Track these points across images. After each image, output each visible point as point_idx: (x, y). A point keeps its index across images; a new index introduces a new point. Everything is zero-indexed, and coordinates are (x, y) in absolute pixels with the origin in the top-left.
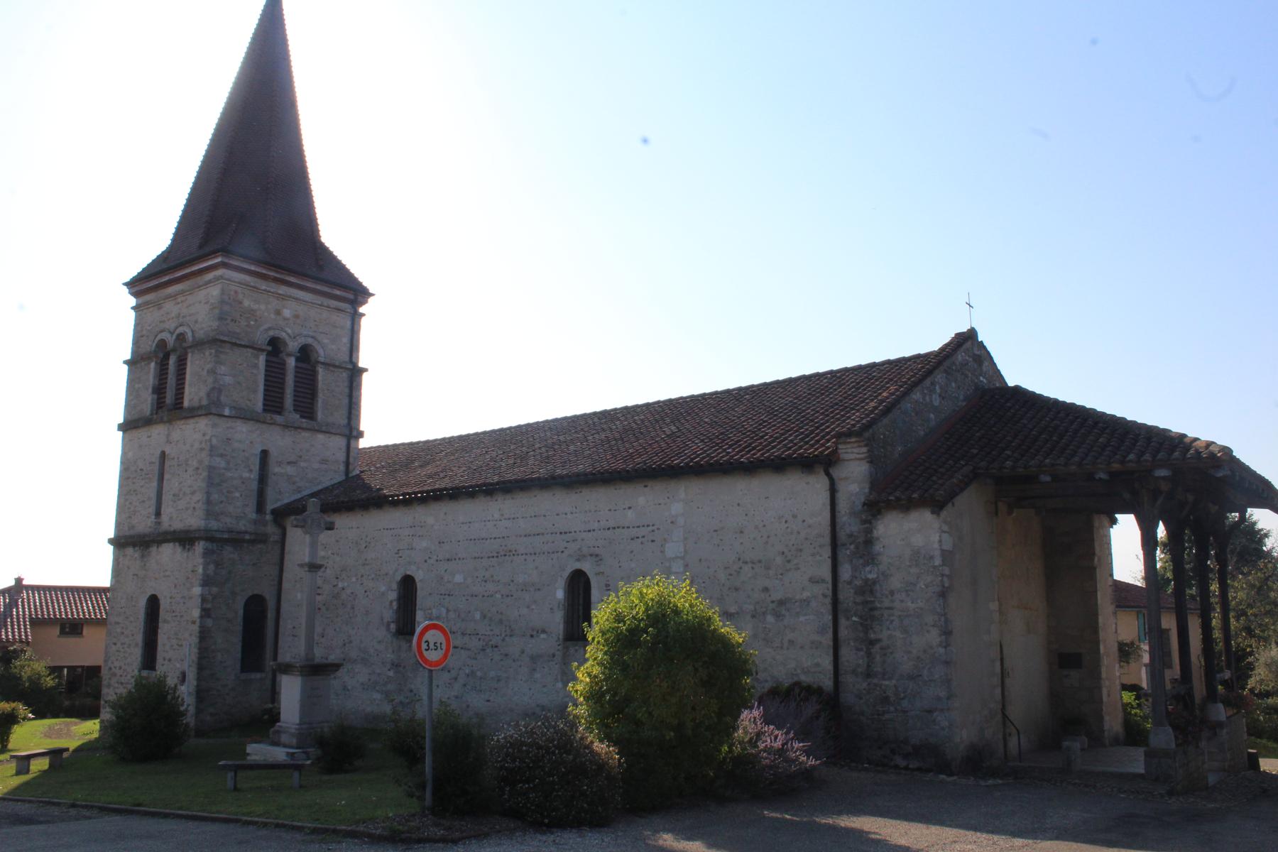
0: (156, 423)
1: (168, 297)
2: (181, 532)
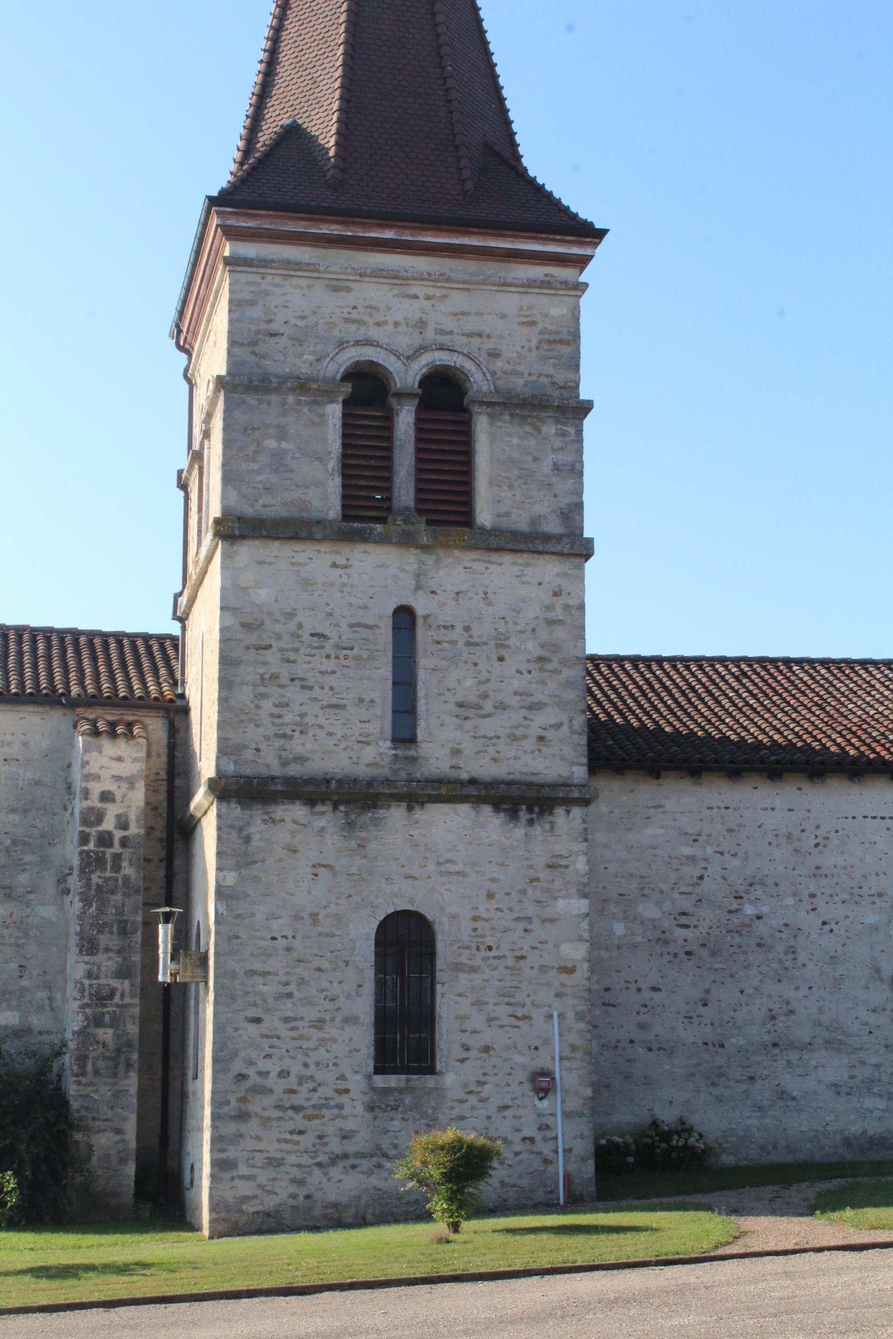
0: (383, 540)
1: (378, 274)
2: (494, 784)
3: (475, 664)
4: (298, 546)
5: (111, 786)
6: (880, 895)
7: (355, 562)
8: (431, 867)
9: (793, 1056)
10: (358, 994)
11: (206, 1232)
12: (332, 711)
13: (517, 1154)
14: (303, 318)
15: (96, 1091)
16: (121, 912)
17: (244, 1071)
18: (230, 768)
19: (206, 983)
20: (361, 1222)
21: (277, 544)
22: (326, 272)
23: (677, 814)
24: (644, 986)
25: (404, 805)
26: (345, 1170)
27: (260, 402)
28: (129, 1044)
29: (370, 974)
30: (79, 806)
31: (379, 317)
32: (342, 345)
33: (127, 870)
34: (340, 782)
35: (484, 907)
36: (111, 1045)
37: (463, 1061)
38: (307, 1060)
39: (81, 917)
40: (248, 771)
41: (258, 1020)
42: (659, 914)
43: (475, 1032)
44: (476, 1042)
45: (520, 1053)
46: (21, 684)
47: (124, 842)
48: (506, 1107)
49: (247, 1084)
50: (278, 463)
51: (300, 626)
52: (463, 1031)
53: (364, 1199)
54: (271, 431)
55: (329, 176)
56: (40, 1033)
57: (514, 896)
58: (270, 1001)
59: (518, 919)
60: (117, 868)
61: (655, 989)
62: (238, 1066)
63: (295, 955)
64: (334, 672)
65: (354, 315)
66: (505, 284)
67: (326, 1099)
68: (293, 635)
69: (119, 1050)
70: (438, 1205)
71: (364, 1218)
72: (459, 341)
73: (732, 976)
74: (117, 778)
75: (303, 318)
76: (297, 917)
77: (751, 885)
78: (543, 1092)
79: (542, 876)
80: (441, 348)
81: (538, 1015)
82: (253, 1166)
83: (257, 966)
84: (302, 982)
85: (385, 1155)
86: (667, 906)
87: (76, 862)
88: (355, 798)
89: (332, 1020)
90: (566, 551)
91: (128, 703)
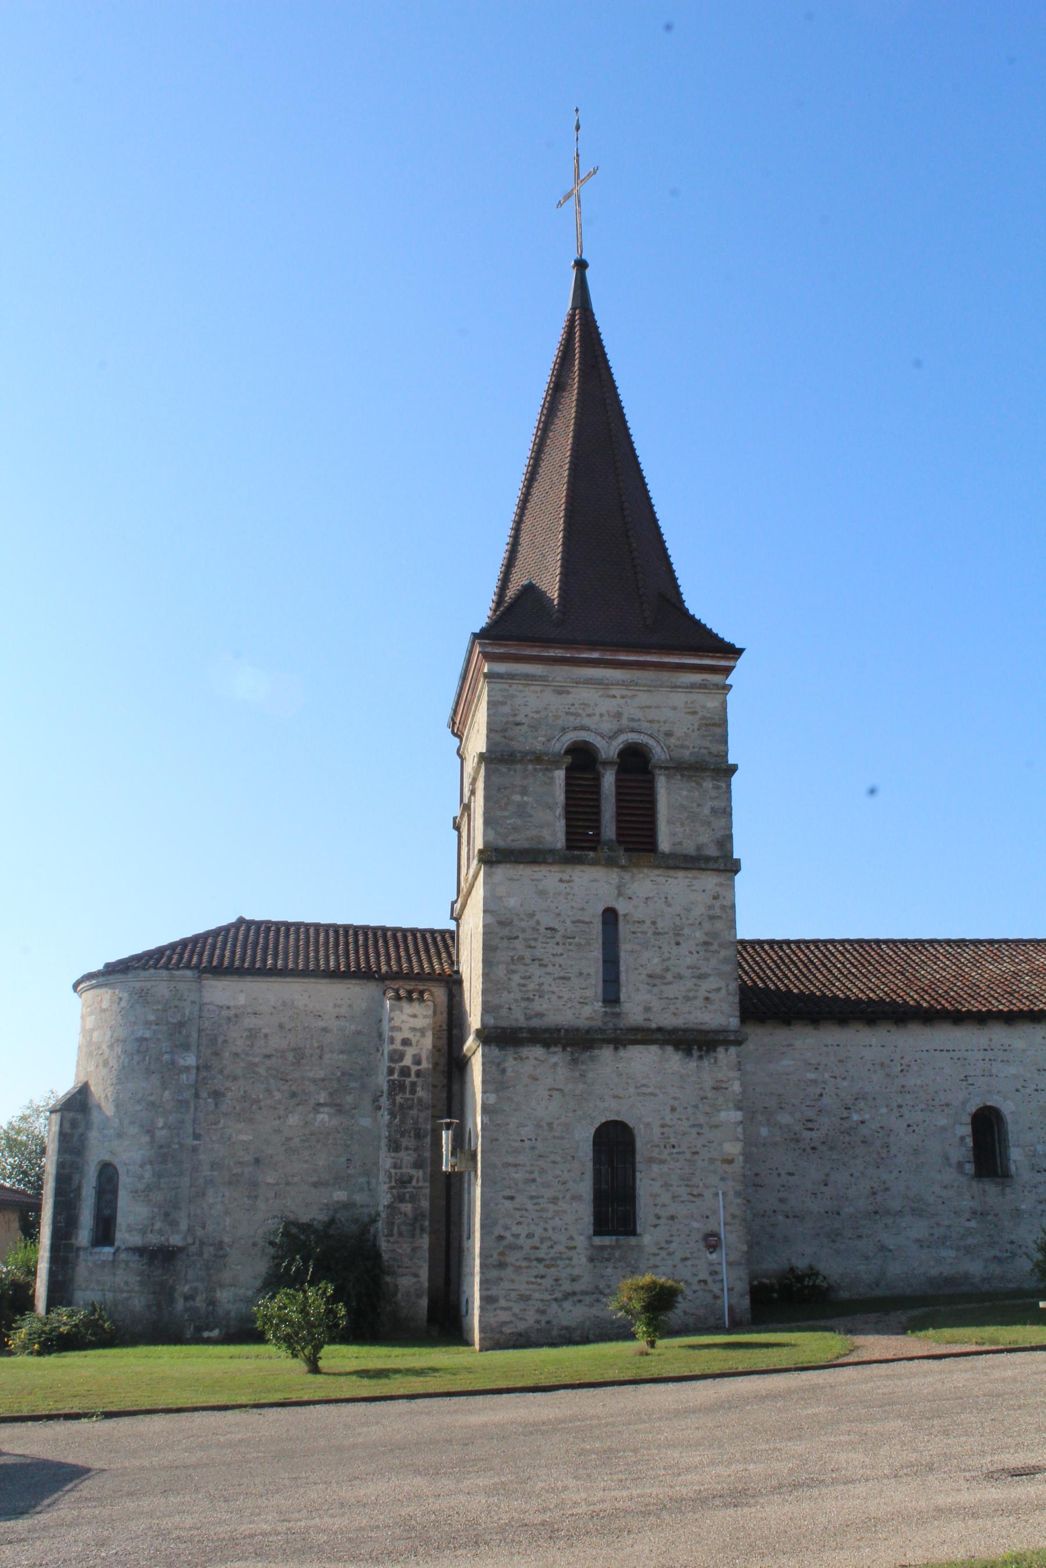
0: (594, 863)
1: (589, 682)
2: (674, 1031)
3: (660, 948)
4: (536, 868)
5: (408, 1035)
6: (947, 1105)
7: (576, 879)
8: (632, 1090)
9: (889, 1221)
10: (582, 1180)
11: (477, 1347)
12: (561, 981)
13: (695, 1292)
14: (538, 712)
15: (401, 1247)
16: (416, 1123)
17: (502, 1234)
18: (491, 1022)
19: (476, 1172)
20: (585, 1340)
21: (522, 866)
22: (553, 681)
23: (803, 1052)
24: (783, 1172)
25: (612, 1046)
26: (574, 1304)
27: (509, 770)
28: (422, 1215)
29: (590, 1166)
30: (387, 1048)
31: (590, 711)
32: (564, 730)
33: (420, 1093)
34: (567, 1031)
35: (668, 1117)
36: (410, 1215)
37: (655, 1226)
38: (546, 1226)
39: (389, 1125)
40: (504, 1024)
41: (512, 1198)
42: (792, 1121)
43: (664, 1205)
44: (664, 1213)
45: (696, 1220)
46: (348, 965)
47: (418, 1074)
48: (686, 1259)
49: (505, 1243)
50: (522, 810)
51: (538, 923)
52: (656, 1205)
53: (588, 1323)
54: (517, 789)
55: (554, 617)
56: (362, 1206)
57: (690, 1110)
58: (520, 1184)
59: (693, 1126)
60: (413, 1092)
61: (791, 1174)
62: (498, 1230)
63: (537, 1152)
64: (562, 955)
65: (573, 710)
66: (676, 687)
67: (560, 1253)
68: (534, 929)
69: (416, 1219)
70: (640, 1328)
71: (588, 1338)
72: (645, 725)
73: (844, 1164)
74: (413, 1029)
75: (538, 712)
76: (538, 1126)
77: (856, 1099)
78: (713, 1247)
79: (709, 1095)
80: (633, 731)
81: (708, 1194)
82: (510, 1300)
83: (511, 1160)
84: (542, 1171)
85: (602, 1293)
86: (798, 1115)
87: (385, 1088)
88: (577, 1042)
89: (564, 1197)
90: (722, 868)
91: (420, 977)
